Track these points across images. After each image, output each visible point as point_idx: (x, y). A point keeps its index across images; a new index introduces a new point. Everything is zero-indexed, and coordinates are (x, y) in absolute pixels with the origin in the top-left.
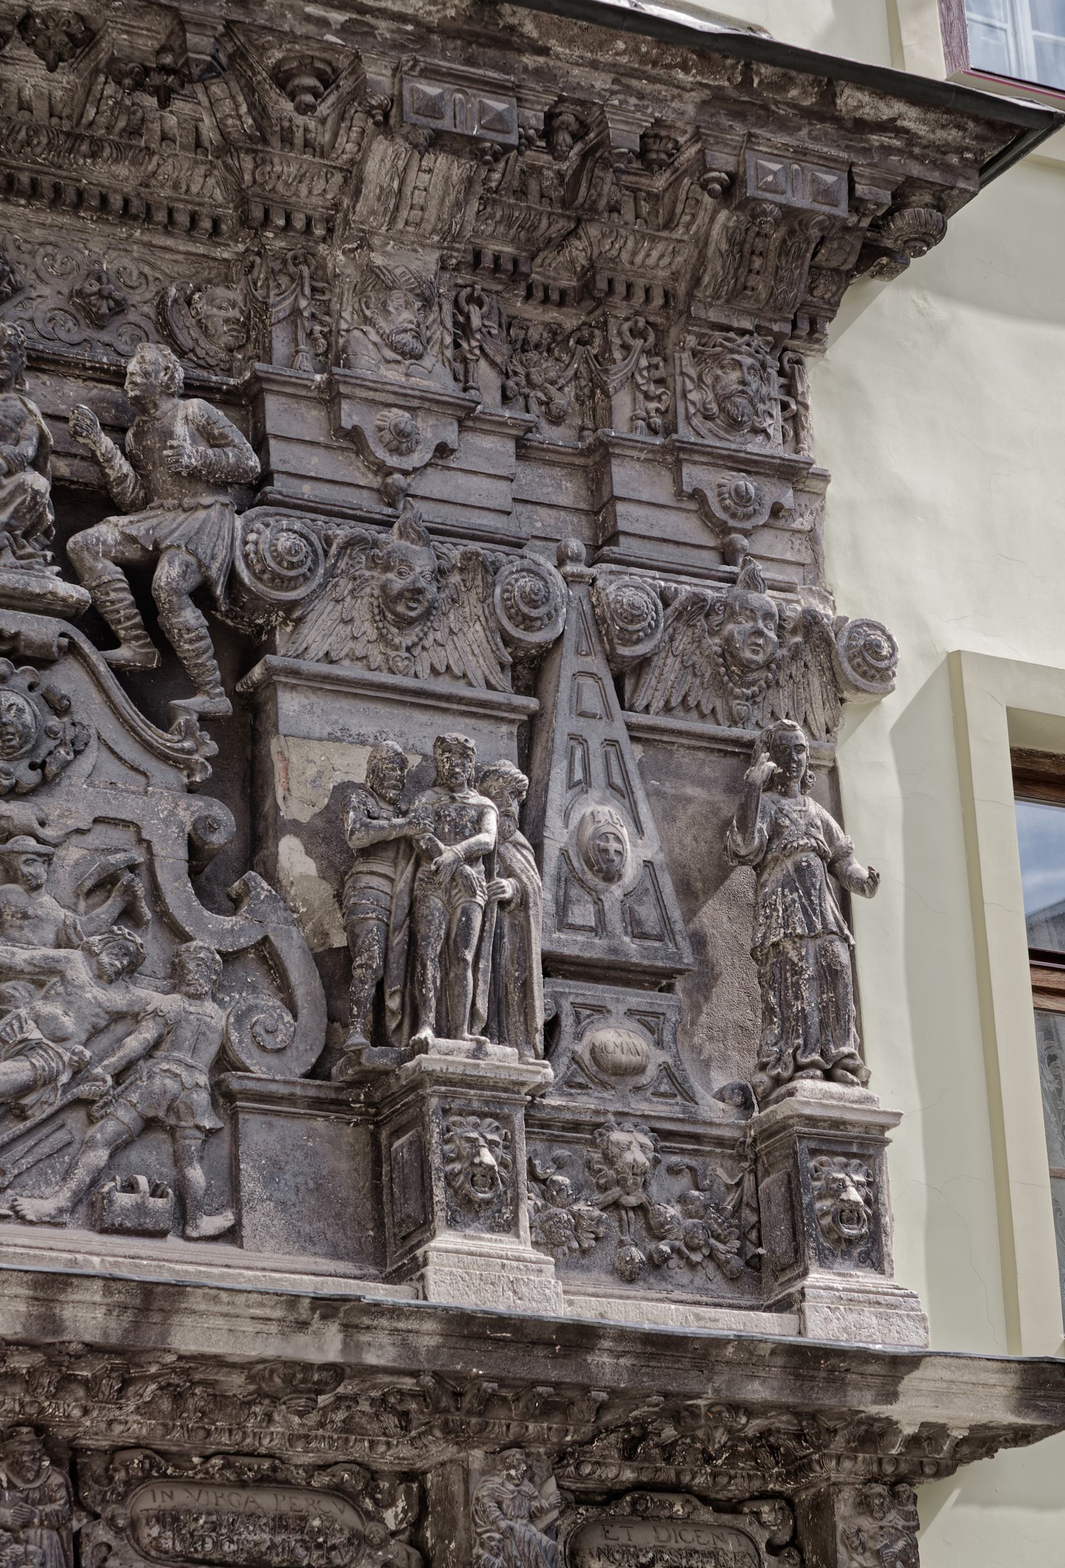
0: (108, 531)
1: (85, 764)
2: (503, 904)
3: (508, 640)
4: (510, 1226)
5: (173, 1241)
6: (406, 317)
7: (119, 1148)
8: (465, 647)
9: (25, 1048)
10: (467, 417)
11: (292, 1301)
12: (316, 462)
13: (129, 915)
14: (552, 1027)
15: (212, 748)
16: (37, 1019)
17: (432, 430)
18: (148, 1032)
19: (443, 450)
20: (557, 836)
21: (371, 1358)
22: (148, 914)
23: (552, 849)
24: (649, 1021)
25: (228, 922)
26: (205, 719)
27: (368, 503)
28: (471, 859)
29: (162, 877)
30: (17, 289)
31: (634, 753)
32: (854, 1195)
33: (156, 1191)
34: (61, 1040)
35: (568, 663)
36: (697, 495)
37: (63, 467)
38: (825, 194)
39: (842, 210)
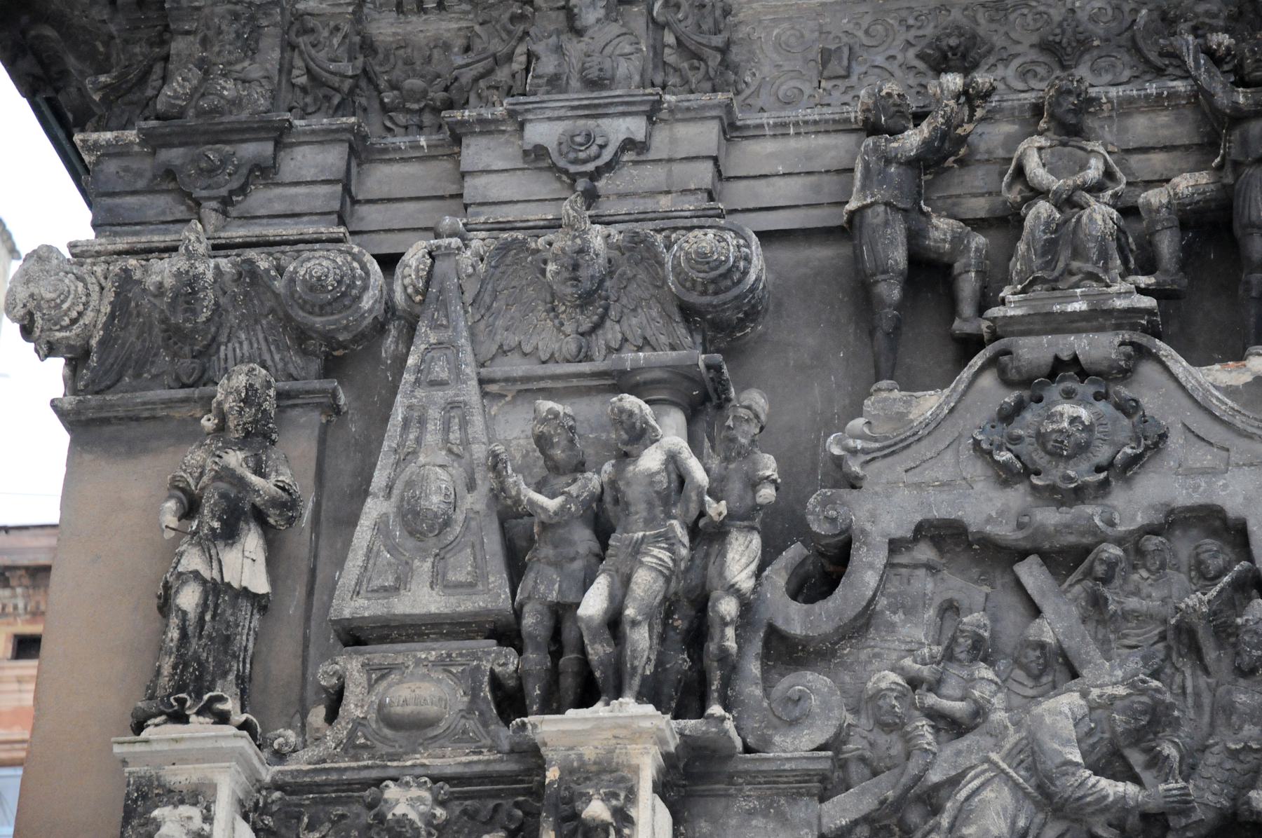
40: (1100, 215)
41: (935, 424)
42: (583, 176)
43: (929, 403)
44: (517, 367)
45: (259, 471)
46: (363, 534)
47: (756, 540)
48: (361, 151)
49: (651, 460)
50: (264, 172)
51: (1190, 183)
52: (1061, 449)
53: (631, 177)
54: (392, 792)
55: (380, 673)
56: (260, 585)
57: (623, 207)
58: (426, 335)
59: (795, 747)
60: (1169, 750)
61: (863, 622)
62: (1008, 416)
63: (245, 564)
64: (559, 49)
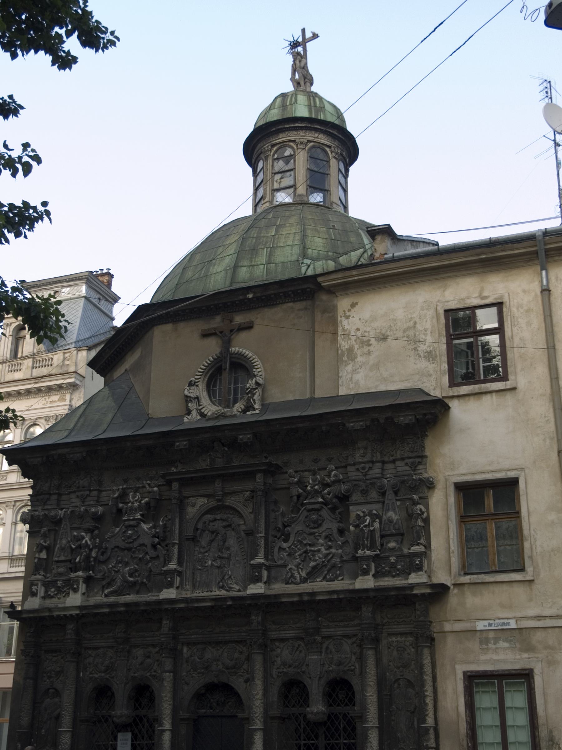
0: (326, 491)
1: (325, 522)
2: (371, 531)
3: (379, 492)
4: (369, 575)
5: (336, 582)
6: (362, 451)
7: (329, 571)
8: (374, 495)
9: (316, 561)
10: (373, 462)
11: (328, 592)
12: (354, 474)
13: (330, 540)
14: (382, 545)
15: (340, 516)
16: (319, 557)
17: (367, 466)
18: (331, 556)
19: (370, 467)
20: (384, 518)
21: (341, 597)
22: (332, 539)
23: (383, 520)
24: (396, 541)
25: (342, 539)
26: (340, 513)
27: (361, 477)
28: (366, 526)
29: (334, 535)
30: (320, 460)
31: (398, 503)
32: (417, 562)
33: (332, 575)
34: (320, 558)
35: (387, 493)
36: (407, 463)
37: (325, 482)
38: (410, 420)
39: (414, 421)
40: (136, 504)
41: (117, 533)
42: (83, 499)
43: (118, 529)
44: (74, 526)
45: (45, 543)
46: (56, 549)
47: (96, 550)
48: (60, 495)
49: (84, 542)
50: (48, 499)
51: (147, 499)
52: (129, 537)
53: (88, 499)
54: (59, 582)
55: (58, 567)
56: (45, 557)
57: (86, 503)
58: (64, 522)
59: (99, 576)
60: (137, 574)
61: (109, 558)
62: (124, 532)
63: (43, 555)
64: (79, 482)
